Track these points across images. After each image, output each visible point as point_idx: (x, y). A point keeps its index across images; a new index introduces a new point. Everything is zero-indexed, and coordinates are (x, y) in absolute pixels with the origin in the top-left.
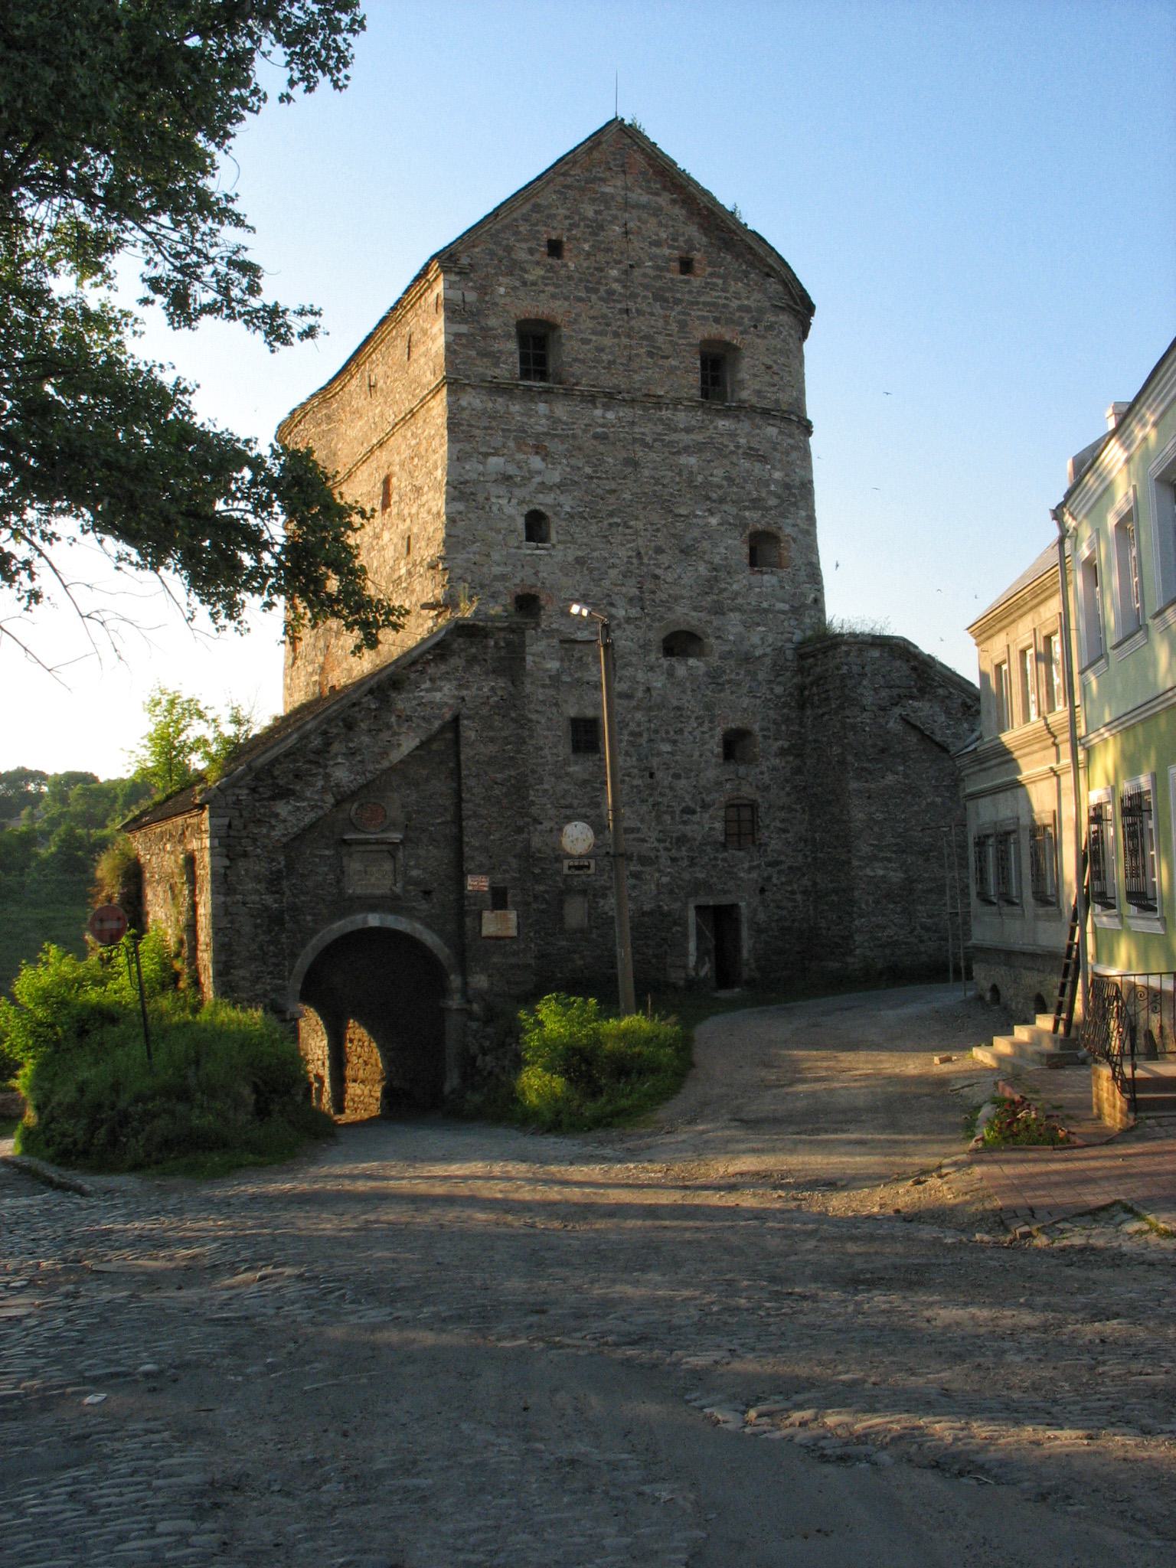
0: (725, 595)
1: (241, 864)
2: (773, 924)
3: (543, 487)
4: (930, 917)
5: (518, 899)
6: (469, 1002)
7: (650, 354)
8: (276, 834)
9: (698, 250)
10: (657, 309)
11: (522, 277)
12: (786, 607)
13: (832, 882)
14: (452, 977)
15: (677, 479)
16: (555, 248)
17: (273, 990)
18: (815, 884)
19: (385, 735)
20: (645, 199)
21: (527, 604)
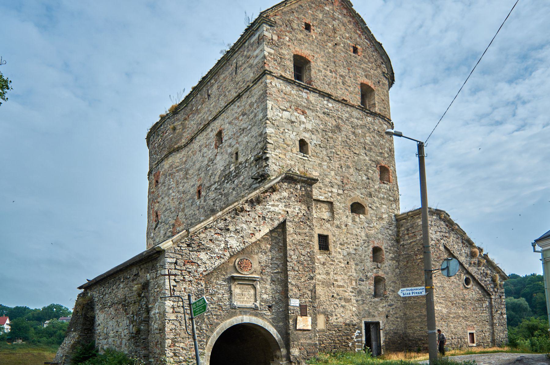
0: (373, 190)
8: (201, 270)
12: (392, 199)
19: (253, 225)
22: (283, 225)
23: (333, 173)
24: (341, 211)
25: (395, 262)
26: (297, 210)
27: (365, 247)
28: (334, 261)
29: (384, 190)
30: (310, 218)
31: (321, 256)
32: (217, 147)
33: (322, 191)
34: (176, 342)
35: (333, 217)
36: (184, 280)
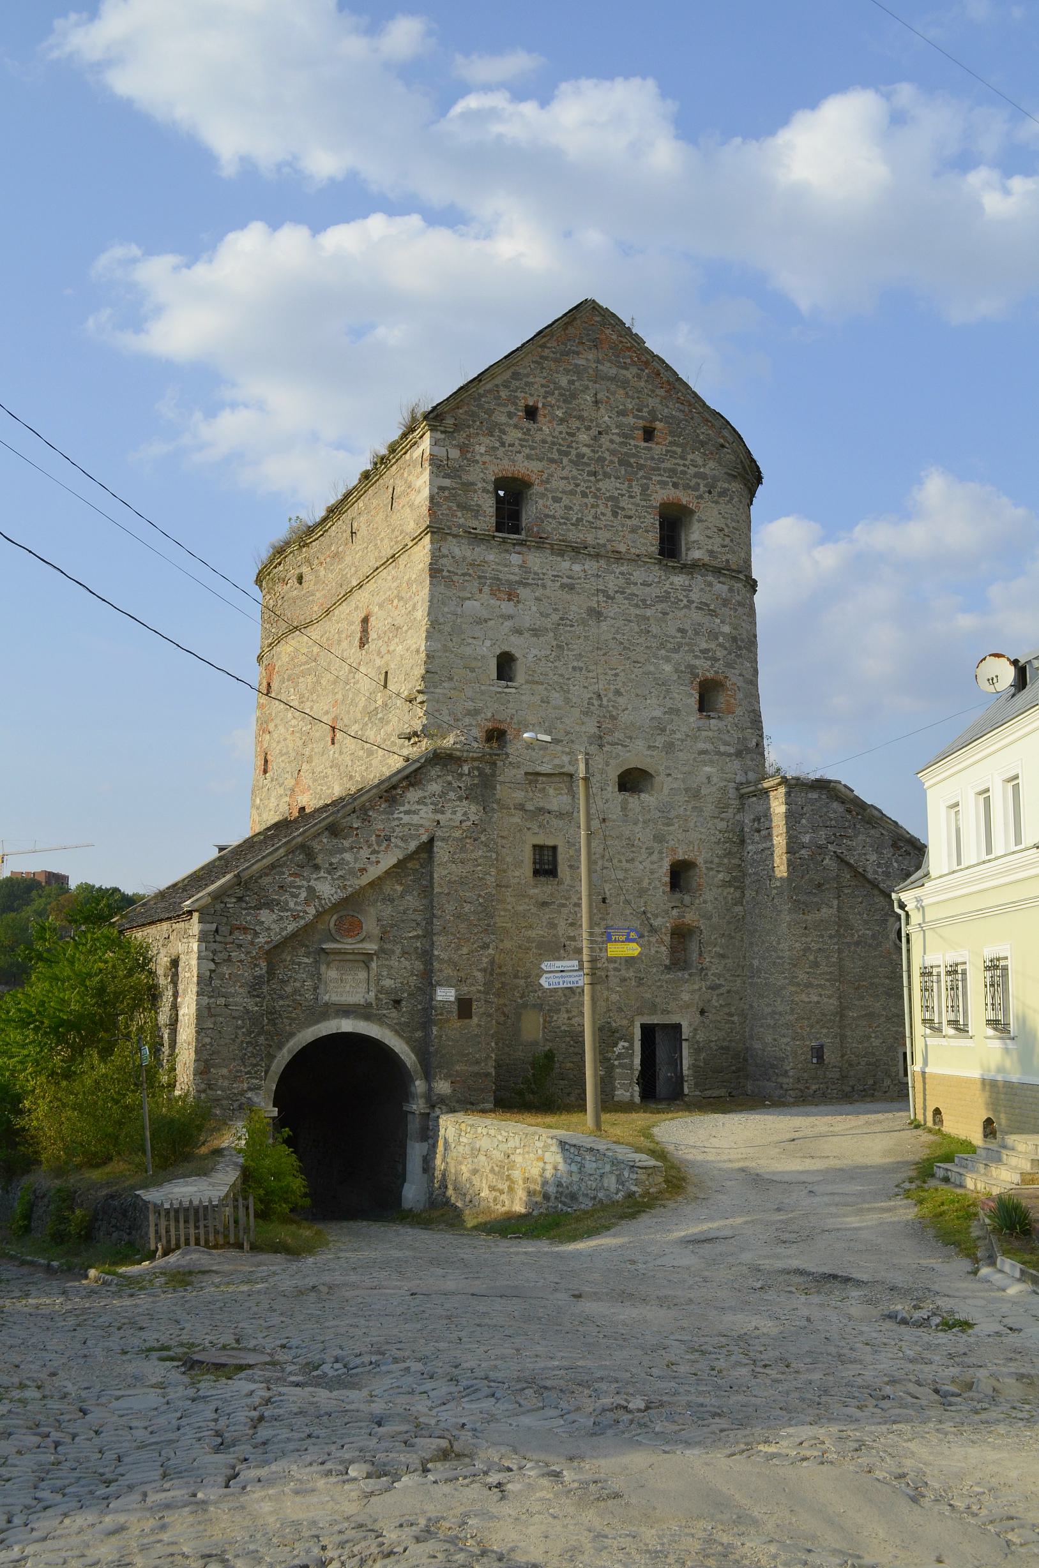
0: (678, 736)
1: (225, 970)
2: (712, 1044)
5: (482, 1010)
6: (433, 1107)
7: (615, 514)
8: (261, 940)
11: (500, 438)
12: (732, 751)
13: (768, 1005)
14: (417, 1083)
15: (636, 629)
17: (250, 1089)
18: (751, 1007)
19: (365, 853)
20: (613, 371)
21: (496, 736)
23: (576, 712)
25: (732, 890)
26: (459, 816)
27: (652, 863)
29: (710, 734)
31: (536, 891)
36: (229, 959)
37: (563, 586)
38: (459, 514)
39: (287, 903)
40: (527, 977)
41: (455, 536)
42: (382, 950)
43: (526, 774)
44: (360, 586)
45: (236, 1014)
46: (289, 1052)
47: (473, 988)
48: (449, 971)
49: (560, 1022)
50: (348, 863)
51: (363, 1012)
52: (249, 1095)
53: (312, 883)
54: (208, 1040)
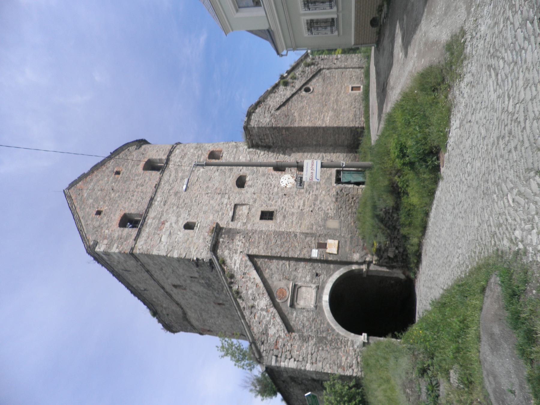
1: (295, 353)
3: (177, 222)
4: (346, 104)
7: (143, 186)
9: (114, 169)
10: (128, 183)
12: (235, 149)
16: (99, 213)
17: (353, 346)
19: (249, 284)
22: (251, 257)
23: (211, 202)
24: (242, 198)
26: (240, 243)
28: (283, 207)
29: (228, 156)
30: (246, 232)
31: (278, 219)
32: (185, 289)
33: (225, 212)
34: (341, 363)
35: (247, 204)
37: (164, 205)
38: (129, 241)
39: (267, 321)
40: (312, 225)
41: (136, 243)
42: (293, 280)
43: (232, 220)
44: (163, 288)
45: (316, 350)
46: (336, 325)
47: (313, 242)
48: (305, 251)
49: (333, 213)
50: (253, 291)
51: (319, 289)
52: (356, 347)
53: (259, 308)
54: (328, 365)
